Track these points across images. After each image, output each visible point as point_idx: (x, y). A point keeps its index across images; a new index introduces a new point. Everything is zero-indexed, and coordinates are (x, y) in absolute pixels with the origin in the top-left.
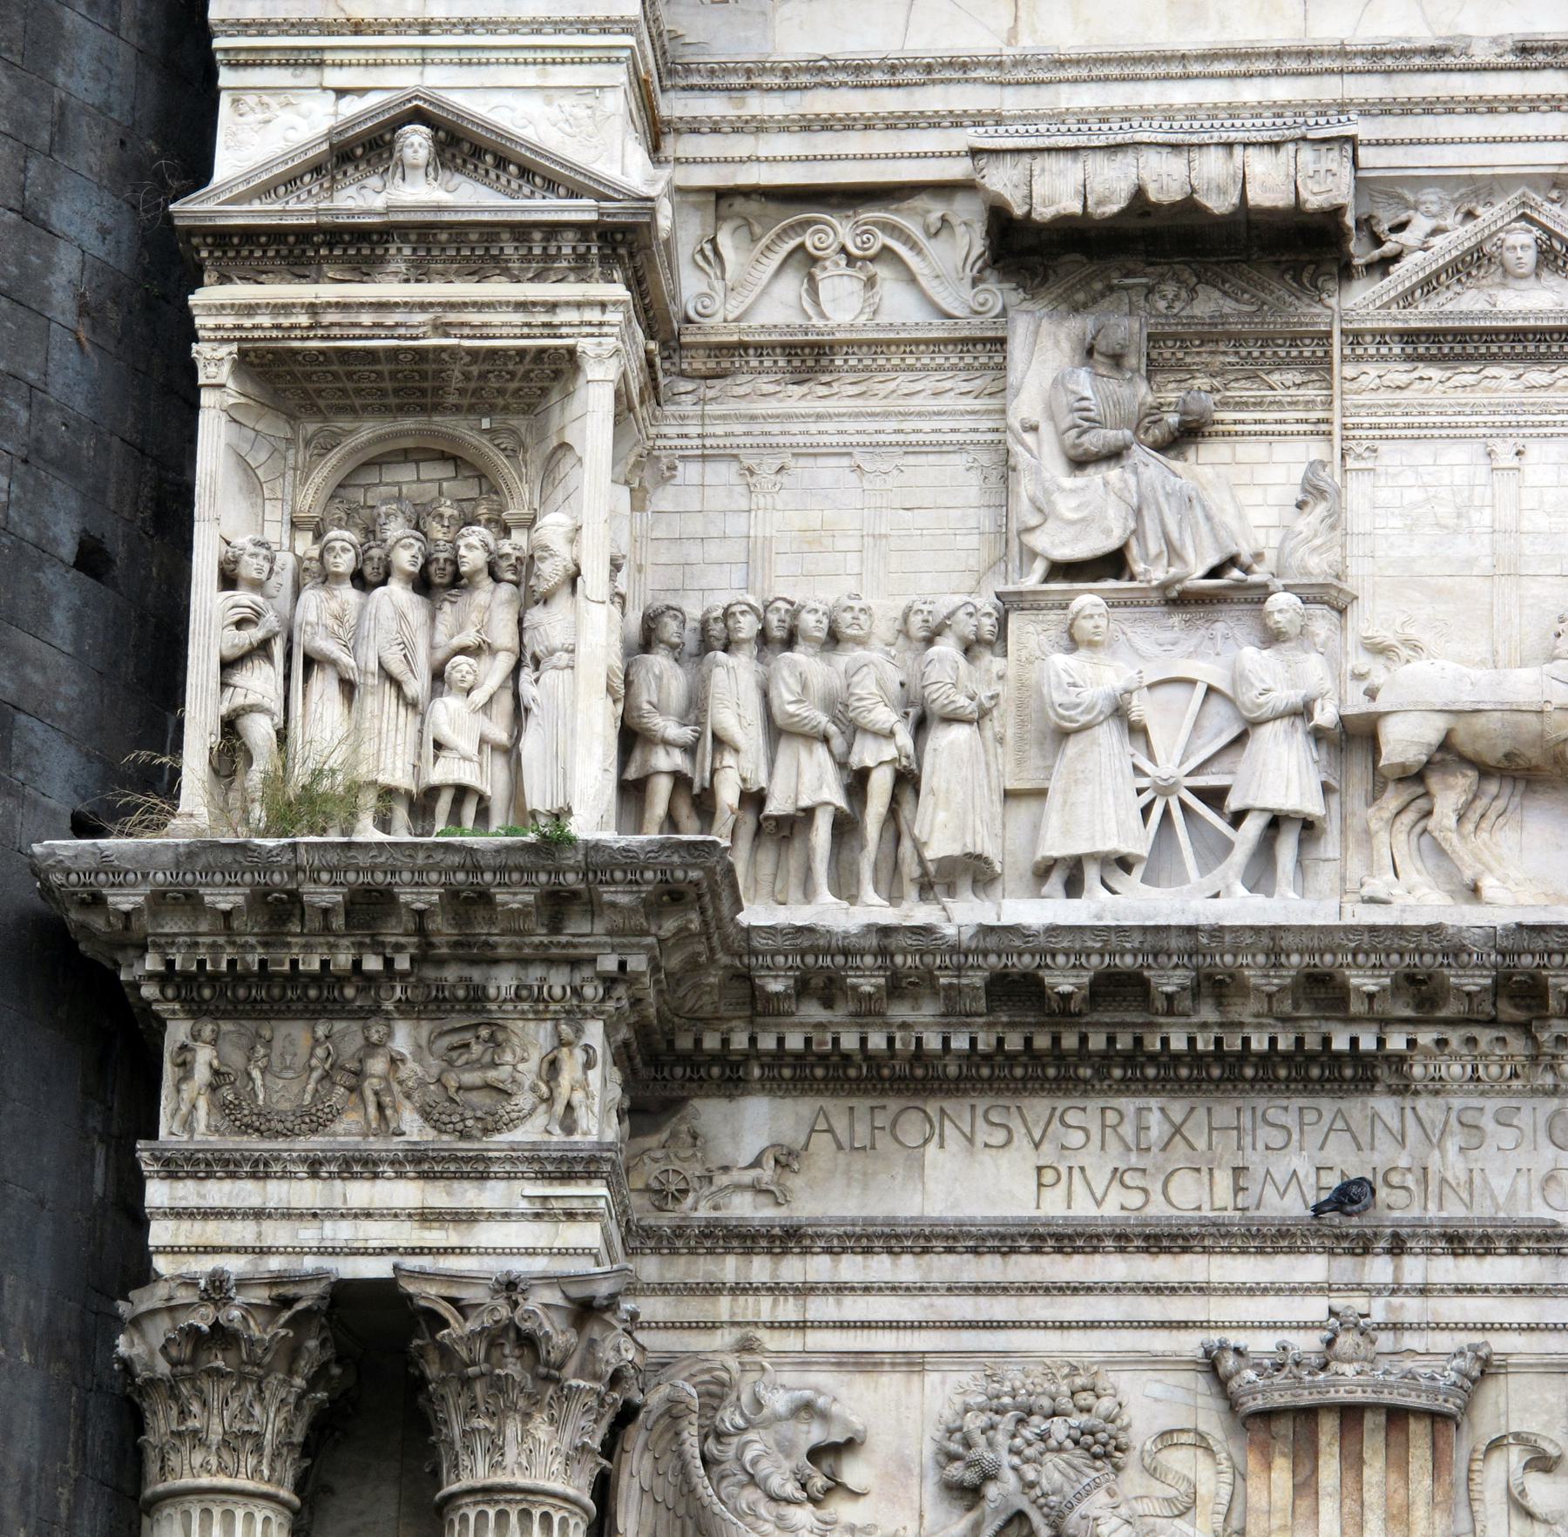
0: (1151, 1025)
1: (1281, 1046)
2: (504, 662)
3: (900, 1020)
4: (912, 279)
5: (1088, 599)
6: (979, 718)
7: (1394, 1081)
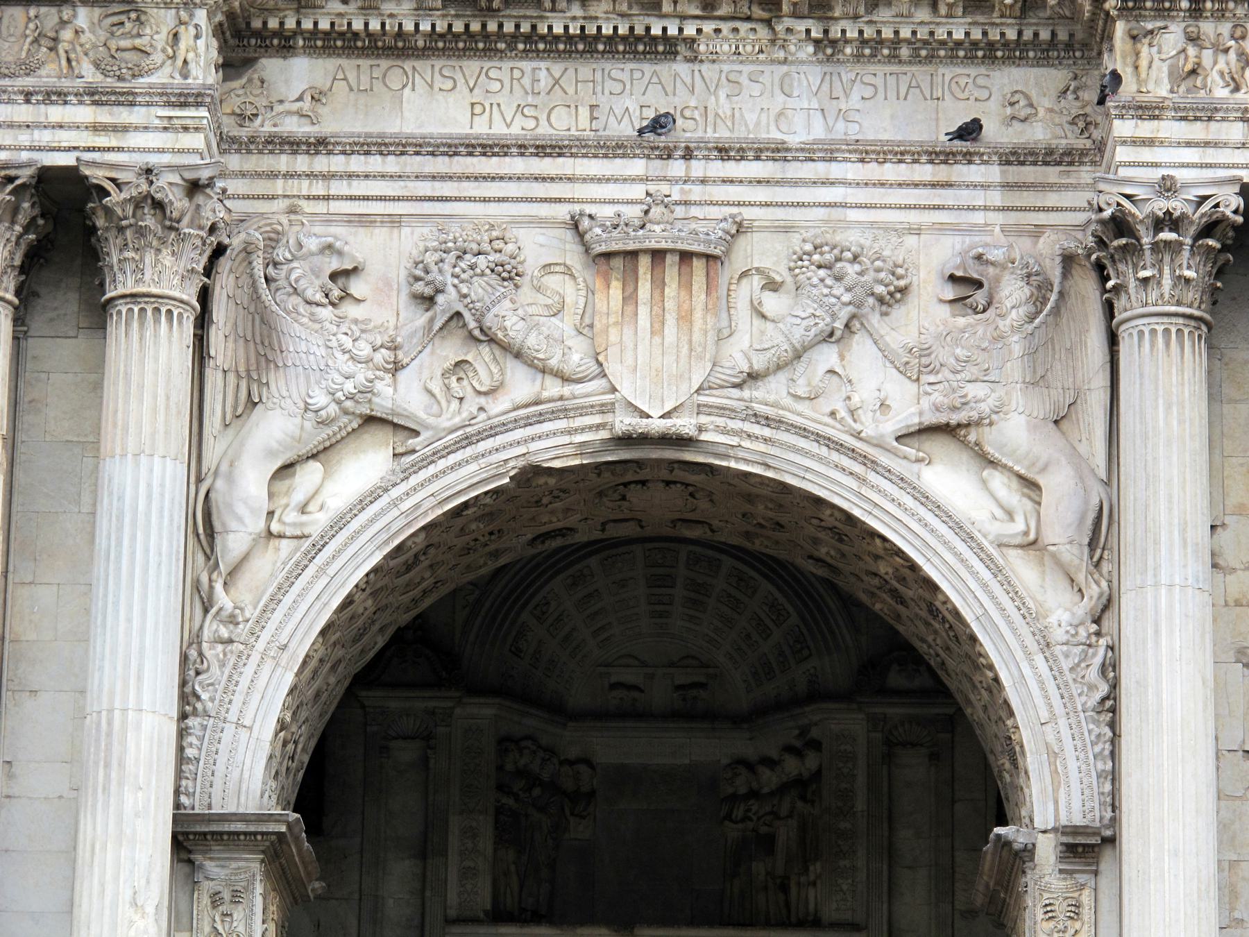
0: (541, 17)
1: (620, 32)
3: (389, 12)
7: (688, 54)
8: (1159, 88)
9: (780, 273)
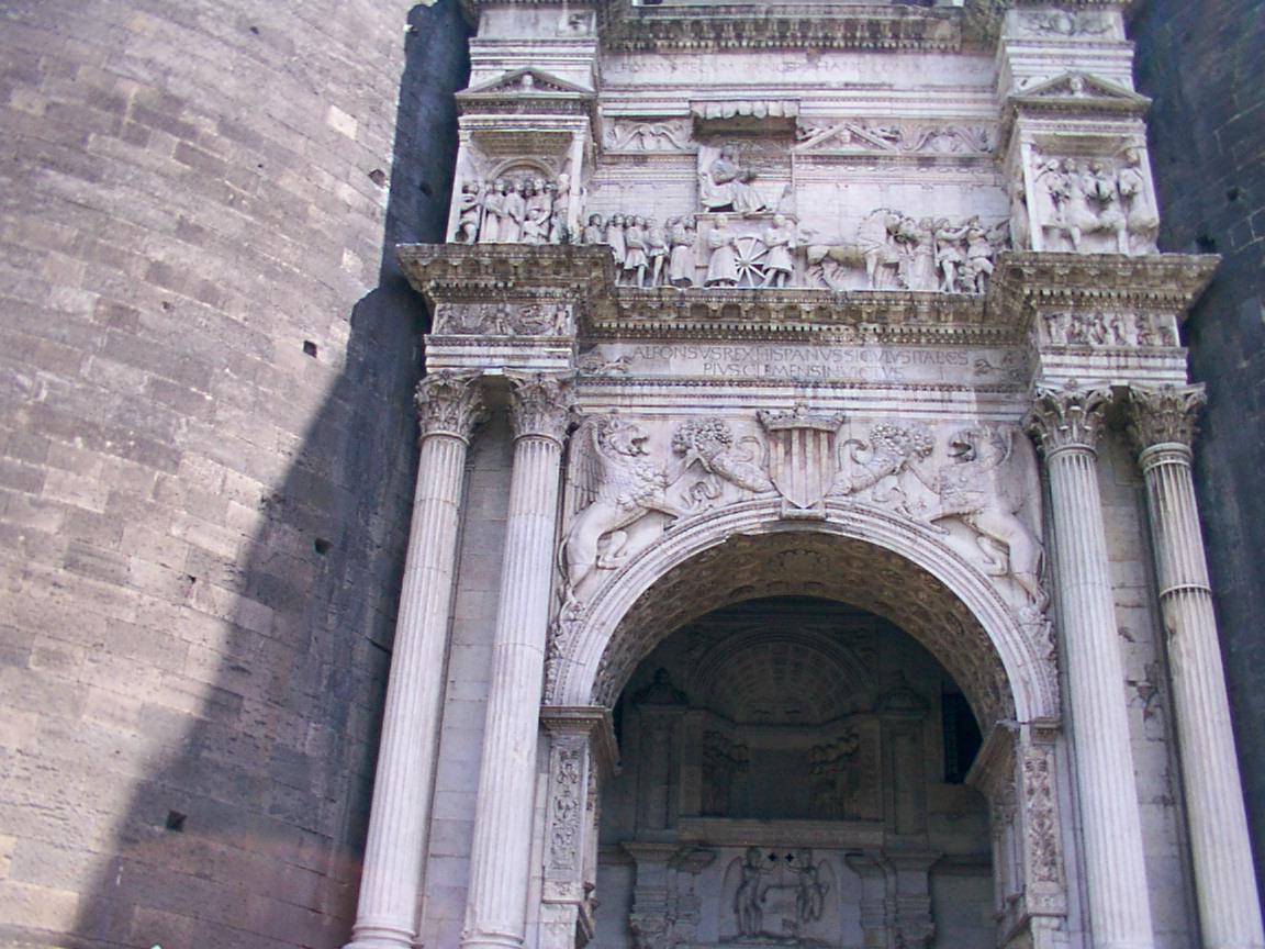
2: (547, 214)
4: (671, 141)
5: (721, 215)
6: (689, 246)
8: (1061, 338)
9: (866, 442)
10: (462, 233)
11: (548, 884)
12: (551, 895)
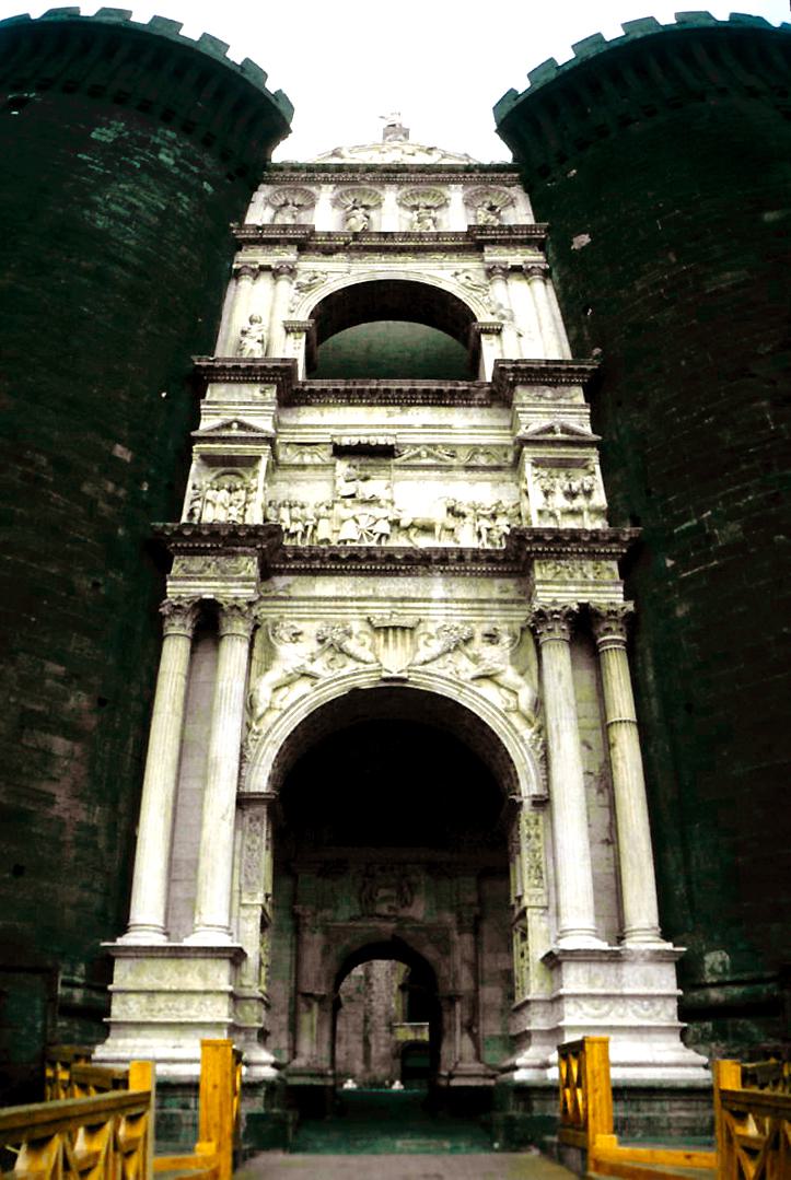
2: (243, 503)
5: (349, 501)
6: (329, 518)
9: (434, 634)
10: (191, 514)
11: (244, 895)
12: (245, 901)
